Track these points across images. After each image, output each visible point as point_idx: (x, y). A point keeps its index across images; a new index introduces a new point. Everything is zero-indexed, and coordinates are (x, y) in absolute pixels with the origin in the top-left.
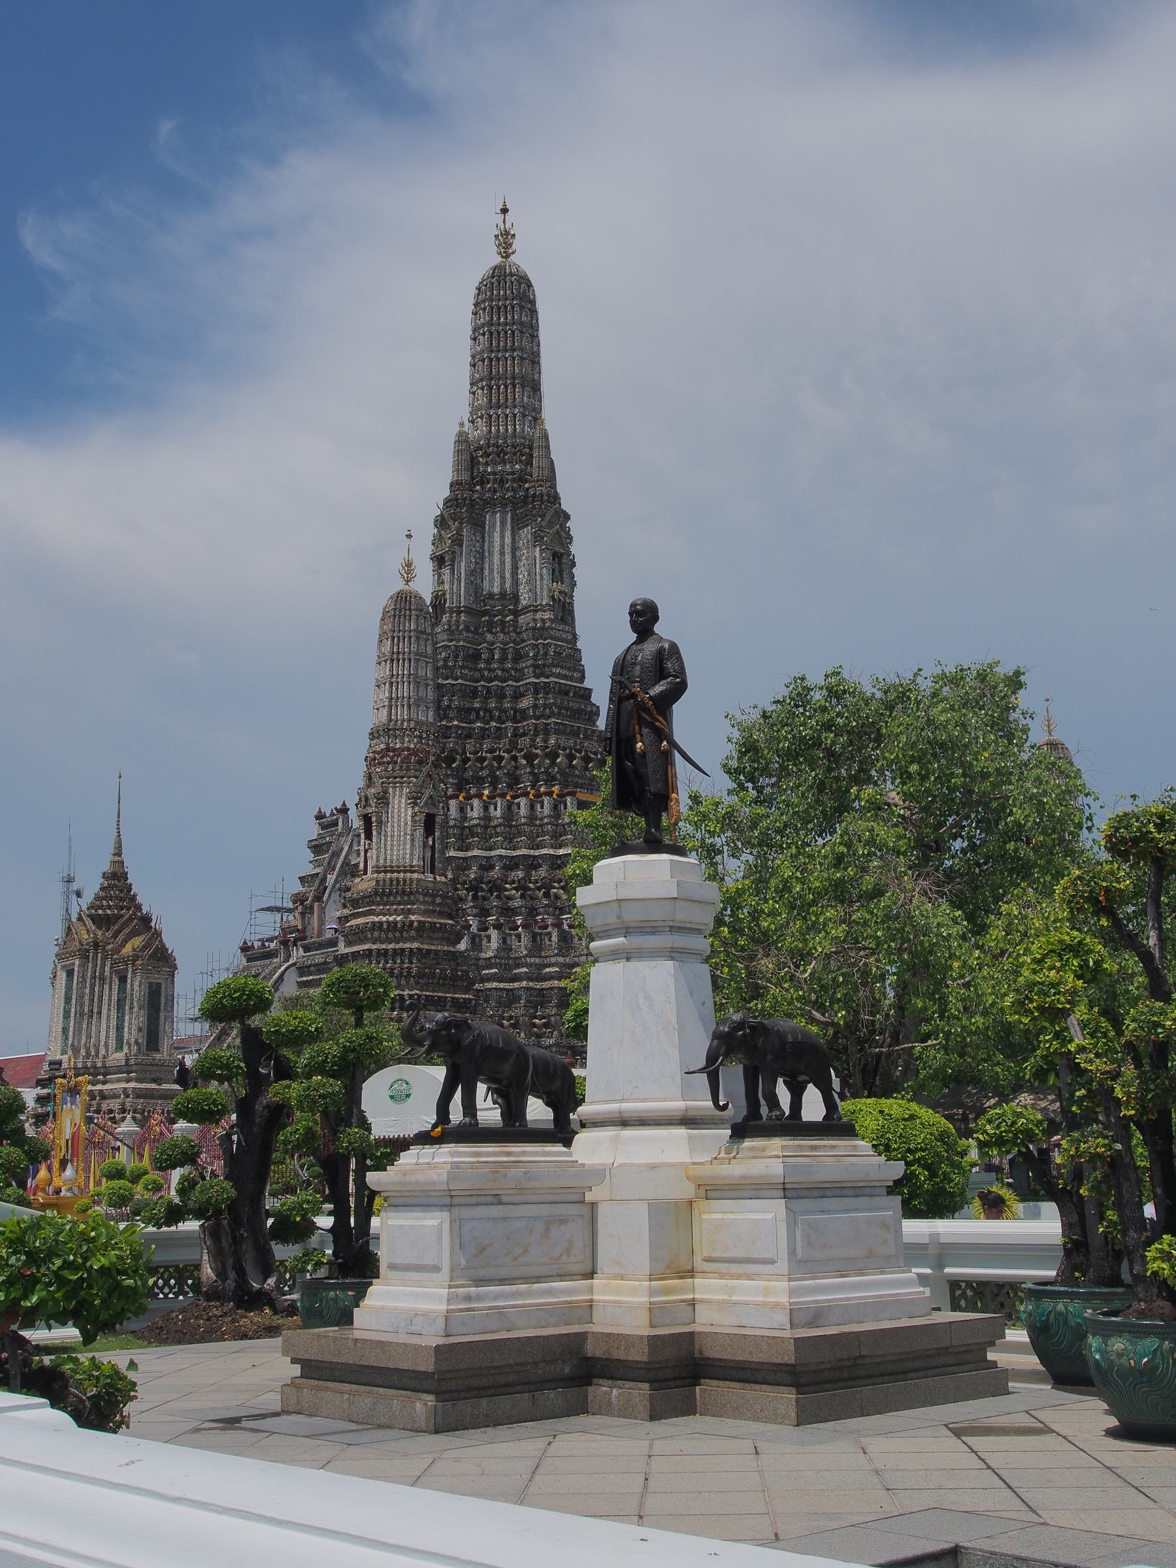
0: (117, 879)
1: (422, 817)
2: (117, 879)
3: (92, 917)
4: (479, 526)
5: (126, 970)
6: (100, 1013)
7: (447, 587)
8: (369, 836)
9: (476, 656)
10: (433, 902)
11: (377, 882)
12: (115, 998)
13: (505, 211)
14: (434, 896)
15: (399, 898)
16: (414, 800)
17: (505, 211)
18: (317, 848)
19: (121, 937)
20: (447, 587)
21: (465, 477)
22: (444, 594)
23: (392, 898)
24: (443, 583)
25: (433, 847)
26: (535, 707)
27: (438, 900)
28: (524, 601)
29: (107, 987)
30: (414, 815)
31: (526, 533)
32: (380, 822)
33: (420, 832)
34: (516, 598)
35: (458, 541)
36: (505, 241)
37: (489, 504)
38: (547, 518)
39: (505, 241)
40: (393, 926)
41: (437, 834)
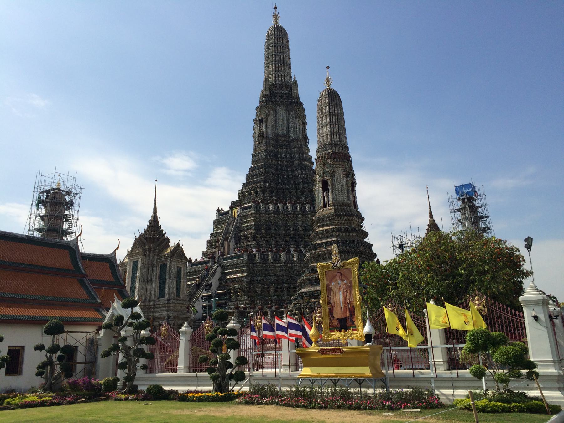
0: (154, 223)
2: (154, 223)
3: (146, 239)
4: (275, 111)
7: (264, 130)
9: (276, 156)
13: (276, 8)
17: (276, 8)
18: (217, 223)
21: (268, 93)
26: (302, 174)
28: (292, 137)
30: (347, 181)
31: (292, 114)
34: (289, 138)
35: (268, 115)
37: (277, 103)
39: (276, 17)
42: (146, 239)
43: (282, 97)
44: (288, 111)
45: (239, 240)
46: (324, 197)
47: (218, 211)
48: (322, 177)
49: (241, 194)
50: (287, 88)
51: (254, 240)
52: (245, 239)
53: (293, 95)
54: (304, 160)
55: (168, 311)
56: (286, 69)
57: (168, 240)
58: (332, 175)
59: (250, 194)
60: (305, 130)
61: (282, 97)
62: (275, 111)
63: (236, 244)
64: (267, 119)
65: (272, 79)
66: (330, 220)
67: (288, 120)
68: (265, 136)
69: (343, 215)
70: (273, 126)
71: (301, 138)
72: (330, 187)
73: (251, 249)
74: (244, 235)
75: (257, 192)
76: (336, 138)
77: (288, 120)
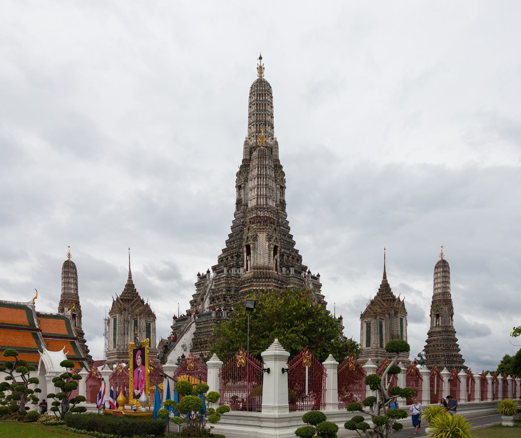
0: (130, 286)
1: (272, 246)
2: (130, 286)
3: (122, 300)
5: (137, 318)
6: (127, 334)
8: (249, 253)
10: (277, 283)
11: (254, 273)
12: (133, 328)
14: (278, 280)
15: (264, 280)
16: (269, 239)
19: (134, 307)
22: (241, 199)
23: (261, 280)
24: (241, 195)
25: (276, 260)
27: (279, 282)
29: (130, 324)
30: (269, 246)
32: (254, 248)
33: (272, 253)
38: (278, 173)
41: (278, 255)
45: (213, 300)
46: (247, 261)
48: (246, 242)
51: (225, 300)
52: (218, 299)
60: (283, 194)
63: (211, 303)
64: (245, 184)
66: (249, 282)
68: (243, 202)
69: (261, 278)
72: (252, 252)
73: (220, 309)
74: (217, 296)
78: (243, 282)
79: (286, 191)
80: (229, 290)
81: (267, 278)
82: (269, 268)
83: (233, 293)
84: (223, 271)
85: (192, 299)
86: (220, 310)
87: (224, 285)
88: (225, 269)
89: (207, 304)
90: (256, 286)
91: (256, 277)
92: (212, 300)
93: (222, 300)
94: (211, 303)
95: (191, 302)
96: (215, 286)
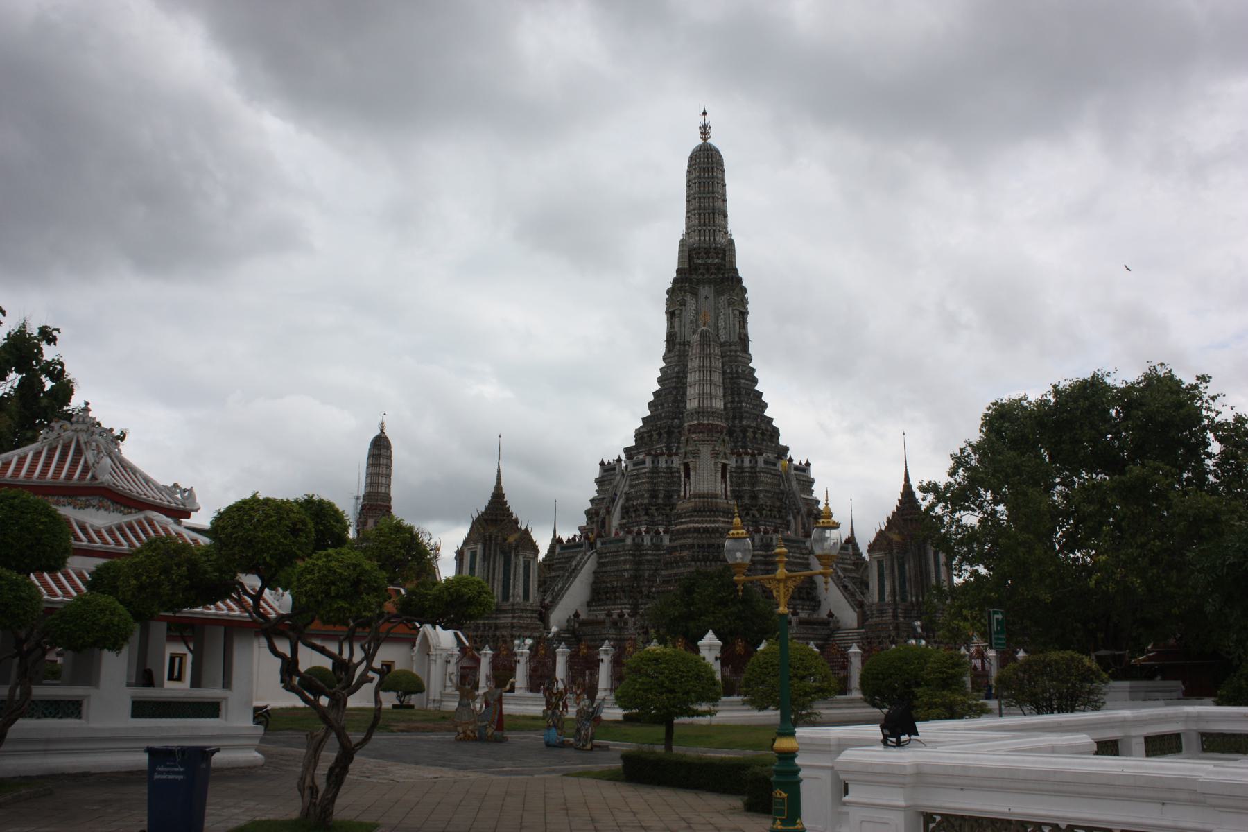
0: (498, 497)
2: (498, 497)
3: (486, 520)
4: (695, 294)
8: (687, 475)
13: (705, 113)
17: (705, 113)
18: (599, 482)
20: (677, 329)
21: (686, 266)
30: (716, 464)
31: (723, 299)
35: (683, 303)
36: (705, 131)
37: (699, 282)
39: (705, 131)
40: (706, 530)
42: (486, 520)
43: (708, 270)
44: (719, 293)
45: (627, 513)
47: (602, 464)
49: (639, 435)
50: (717, 253)
51: (647, 514)
53: (728, 266)
54: (738, 378)
55: (513, 617)
56: (718, 219)
57: (516, 521)
58: (696, 454)
59: (651, 436)
60: (743, 323)
61: (708, 270)
62: (695, 294)
65: (694, 239)
67: (717, 308)
68: (678, 340)
70: (692, 322)
71: (737, 339)
72: (692, 473)
75: (660, 434)
76: (706, 403)
77: (717, 308)
78: (679, 516)
79: (750, 319)
80: (654, 495)
81: (711, 511)
82: (715, 496)
83: (660, 501)
84: (643, 462)
85: (589, 506)
86: (639, 533)
87: (646, 486)
88: (648, 460)
89: (616, 520)
90: (698, 522)
91: (697, 511)
92: (625, 511)
93: (642, 513)
94: (623, 518)
95: (588, 512)
96: (631, 486)
